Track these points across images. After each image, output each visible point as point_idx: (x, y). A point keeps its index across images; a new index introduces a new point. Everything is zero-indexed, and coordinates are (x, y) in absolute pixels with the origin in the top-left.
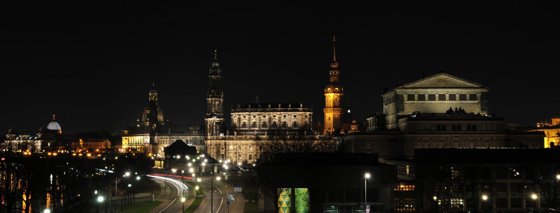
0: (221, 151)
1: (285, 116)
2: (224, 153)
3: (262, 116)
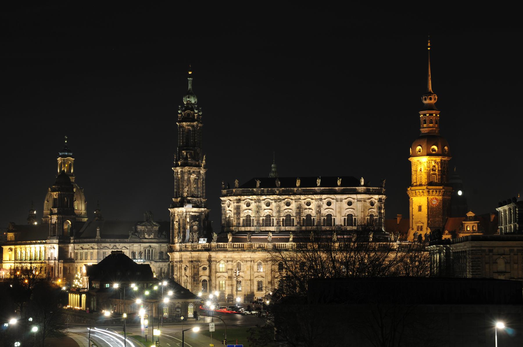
0: (201, 273)
1: (329, 204)
2: (206, 278)
3: (282, 204)
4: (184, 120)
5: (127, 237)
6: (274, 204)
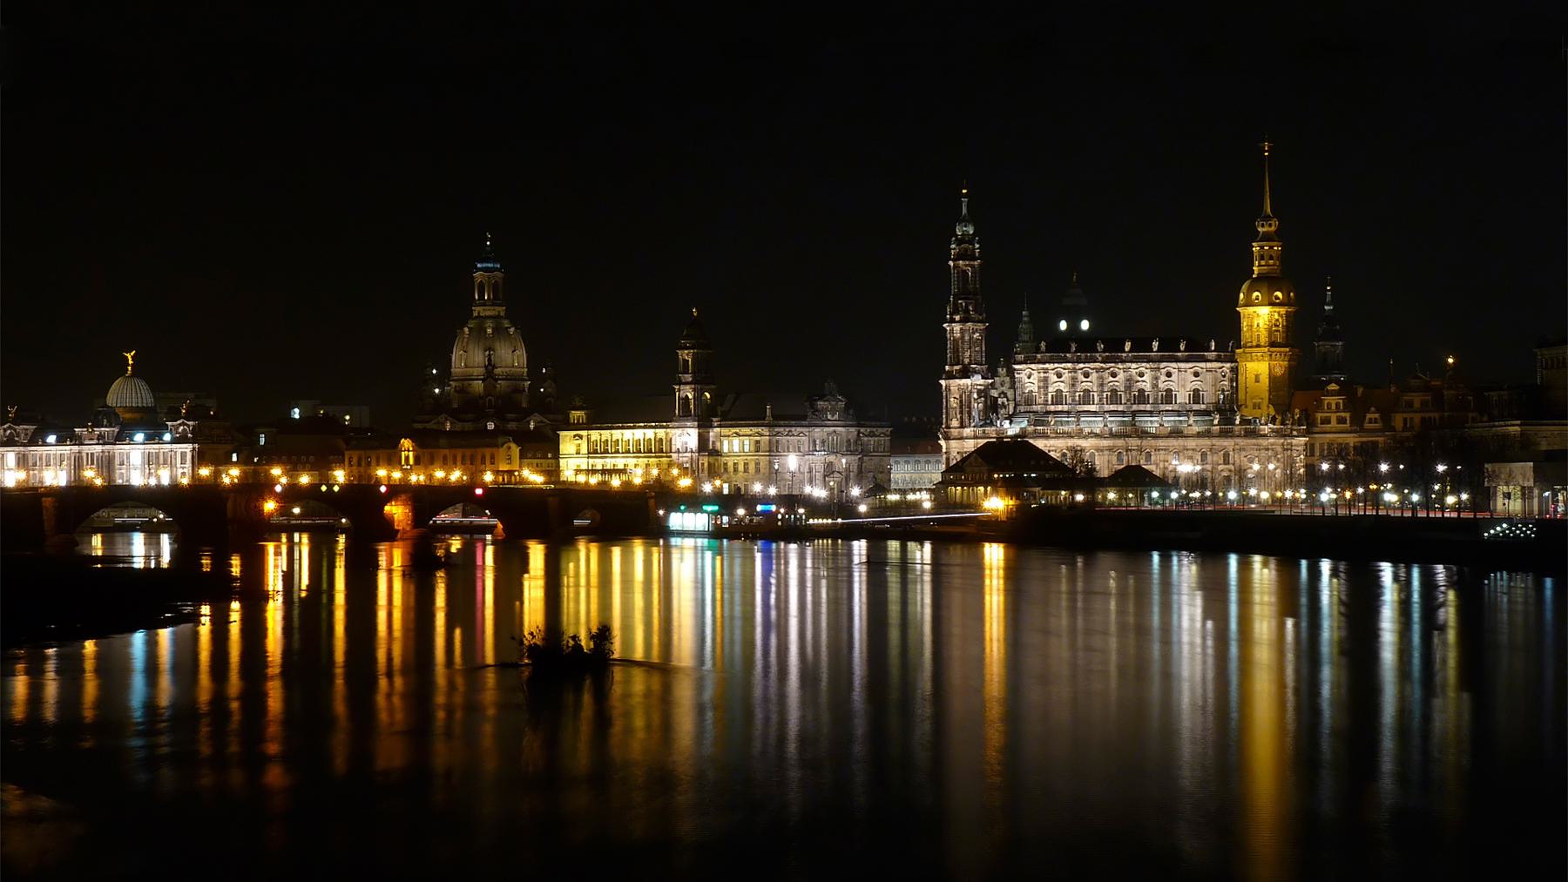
4: (958, 257)
5: (804, 418)
6: (1094, 376)
